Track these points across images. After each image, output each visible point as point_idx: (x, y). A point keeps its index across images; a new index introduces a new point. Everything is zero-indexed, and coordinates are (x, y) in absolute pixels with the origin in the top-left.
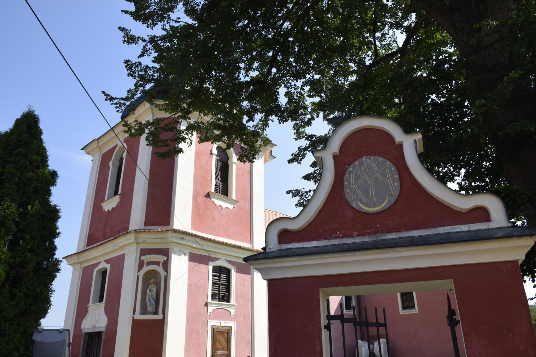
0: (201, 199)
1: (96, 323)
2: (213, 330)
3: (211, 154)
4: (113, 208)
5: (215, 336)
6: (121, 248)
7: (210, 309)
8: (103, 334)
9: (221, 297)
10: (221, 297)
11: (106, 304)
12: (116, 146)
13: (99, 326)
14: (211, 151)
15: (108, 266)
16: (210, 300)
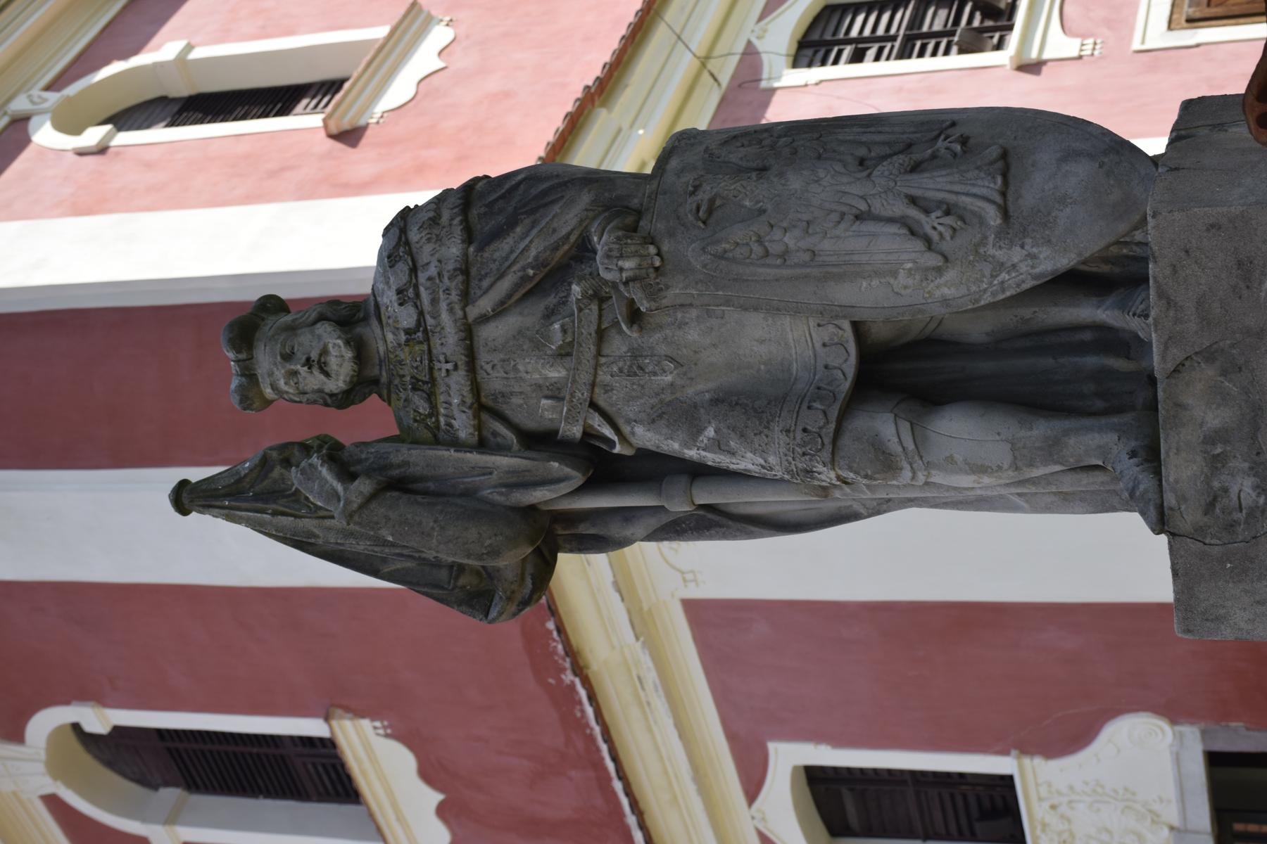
0: (360, 160)
1: (1155, 818)
2: (1192, 21)
3: (102, 150)
4: (428, 774)
5: (1236, 10)
6: (643, 624)
7: (1059, 45)
8: (1222, 745)
9: (989, 23)
10: (989, 23)
11: (1026, 748)
12: (53, 802)
13: (1171, 792)
14: (81, 153)
15: (788, 757)
16: (1003, 58)
